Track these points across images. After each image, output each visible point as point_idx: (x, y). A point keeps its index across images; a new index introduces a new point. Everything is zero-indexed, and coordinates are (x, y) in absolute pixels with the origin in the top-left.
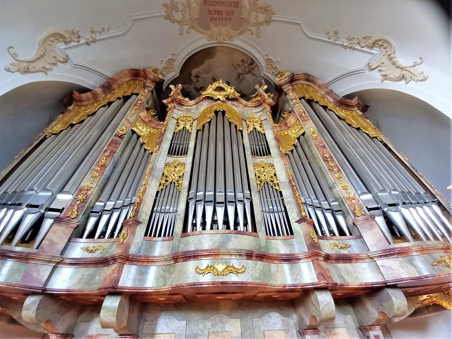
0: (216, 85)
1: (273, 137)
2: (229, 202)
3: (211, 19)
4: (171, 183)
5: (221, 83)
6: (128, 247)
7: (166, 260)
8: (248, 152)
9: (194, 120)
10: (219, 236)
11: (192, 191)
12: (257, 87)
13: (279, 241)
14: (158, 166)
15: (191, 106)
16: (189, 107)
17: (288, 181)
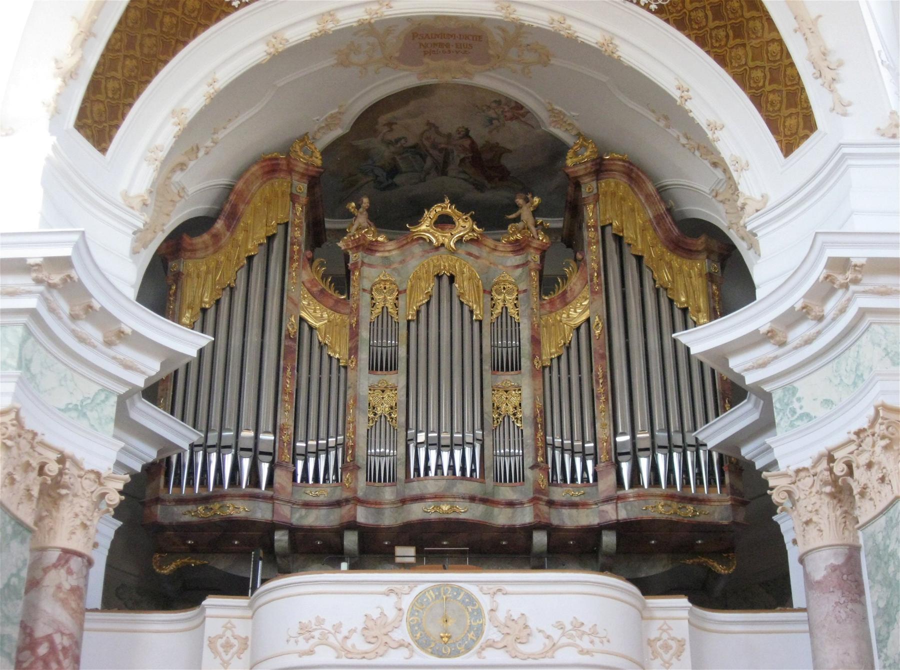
0: (437, 210)
1: (530, 336)
2: (456, 445)
3: (425, 53)
4: (381, 416)
5: (446, 208)
6: (355, 491)
7: (393, 503)
8: (487, 367)
9: (400, 292)
10: (444, 482)
11: (411, 432)
12: (520, 201)
13: (508, 488)
14: (361, 394)
15: (389, 251)
16: (387, 254)
17: (532, 416)
